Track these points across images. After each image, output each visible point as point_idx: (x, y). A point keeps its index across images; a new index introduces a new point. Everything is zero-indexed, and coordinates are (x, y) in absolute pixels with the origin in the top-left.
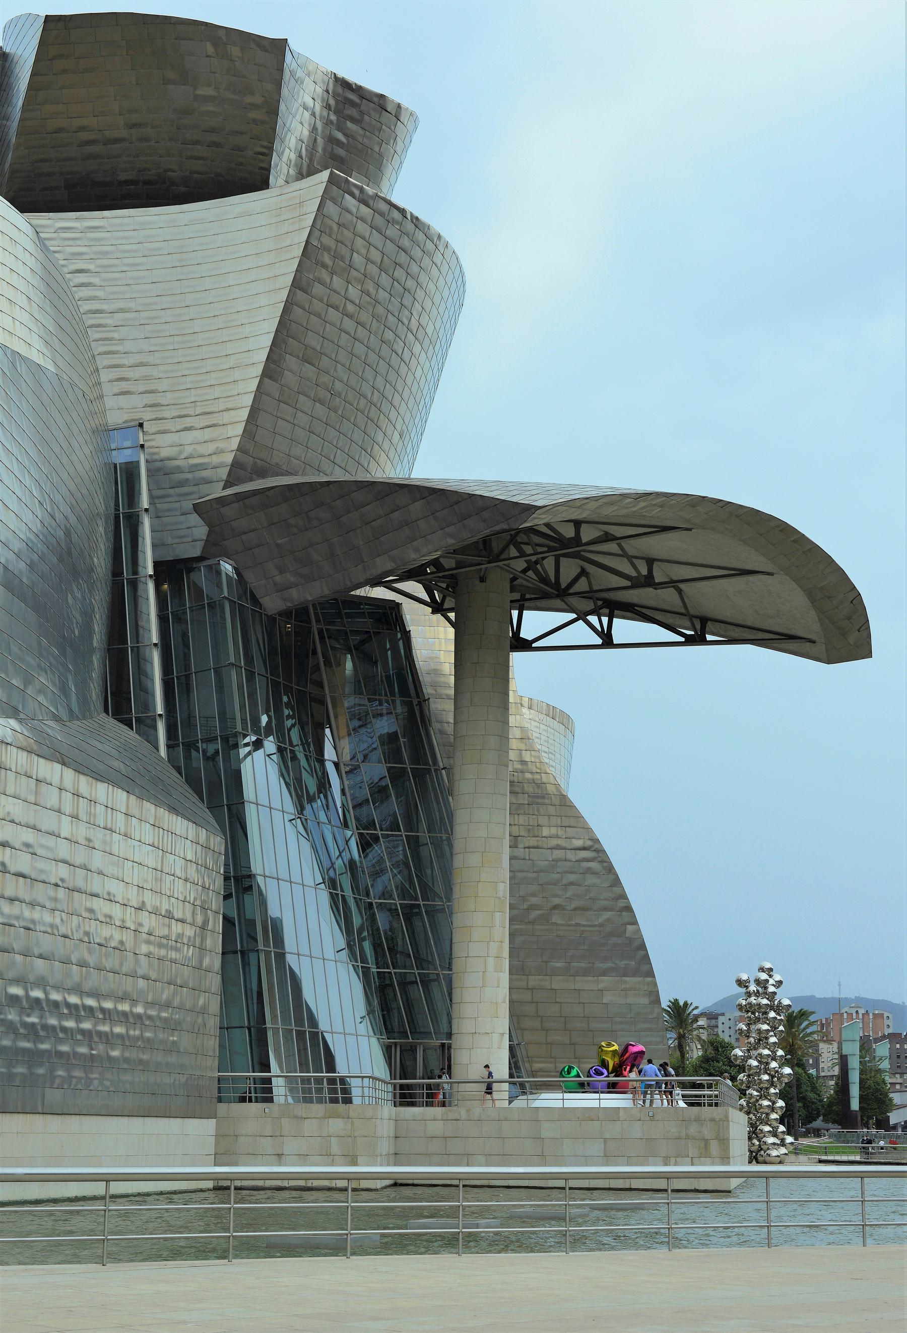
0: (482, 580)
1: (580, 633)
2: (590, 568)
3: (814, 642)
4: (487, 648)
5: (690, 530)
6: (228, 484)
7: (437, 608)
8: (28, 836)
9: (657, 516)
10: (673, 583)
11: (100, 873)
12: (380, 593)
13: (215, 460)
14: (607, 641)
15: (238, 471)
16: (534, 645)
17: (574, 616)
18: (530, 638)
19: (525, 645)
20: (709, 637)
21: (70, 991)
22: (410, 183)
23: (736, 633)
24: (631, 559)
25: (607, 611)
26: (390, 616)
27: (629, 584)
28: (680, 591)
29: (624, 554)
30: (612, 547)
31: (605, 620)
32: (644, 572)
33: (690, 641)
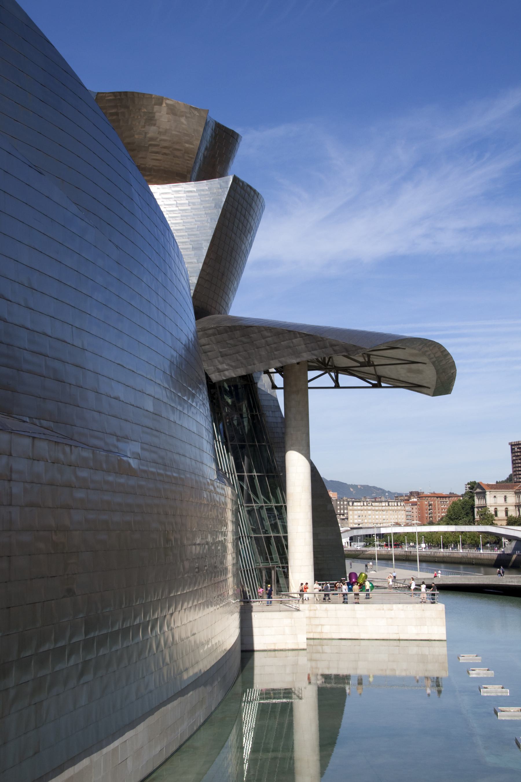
5: (405, 349)
14: (337, 386)
27: (359, 365)
32: (367, 359)
33: (374, 386)
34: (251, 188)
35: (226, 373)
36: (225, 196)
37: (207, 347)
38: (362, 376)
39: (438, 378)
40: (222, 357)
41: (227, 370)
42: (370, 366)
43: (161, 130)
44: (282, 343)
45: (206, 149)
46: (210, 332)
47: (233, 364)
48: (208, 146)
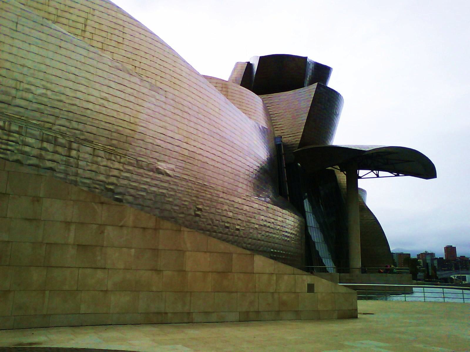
1: (372, 174)
4: (353, 179)
6: (299, 148)
7: (342, 170)
8: (273, 221)
11: (284, 227)
12: (330, 168)
14: (378, 176)
16: (362, 177)
17: (371, 171)
18: (361, 176)
19: (360, 178)
20: (400, 175)
21: (279, 250)
22: (332, 83)
26: (333, 172)
33: (396, 176)
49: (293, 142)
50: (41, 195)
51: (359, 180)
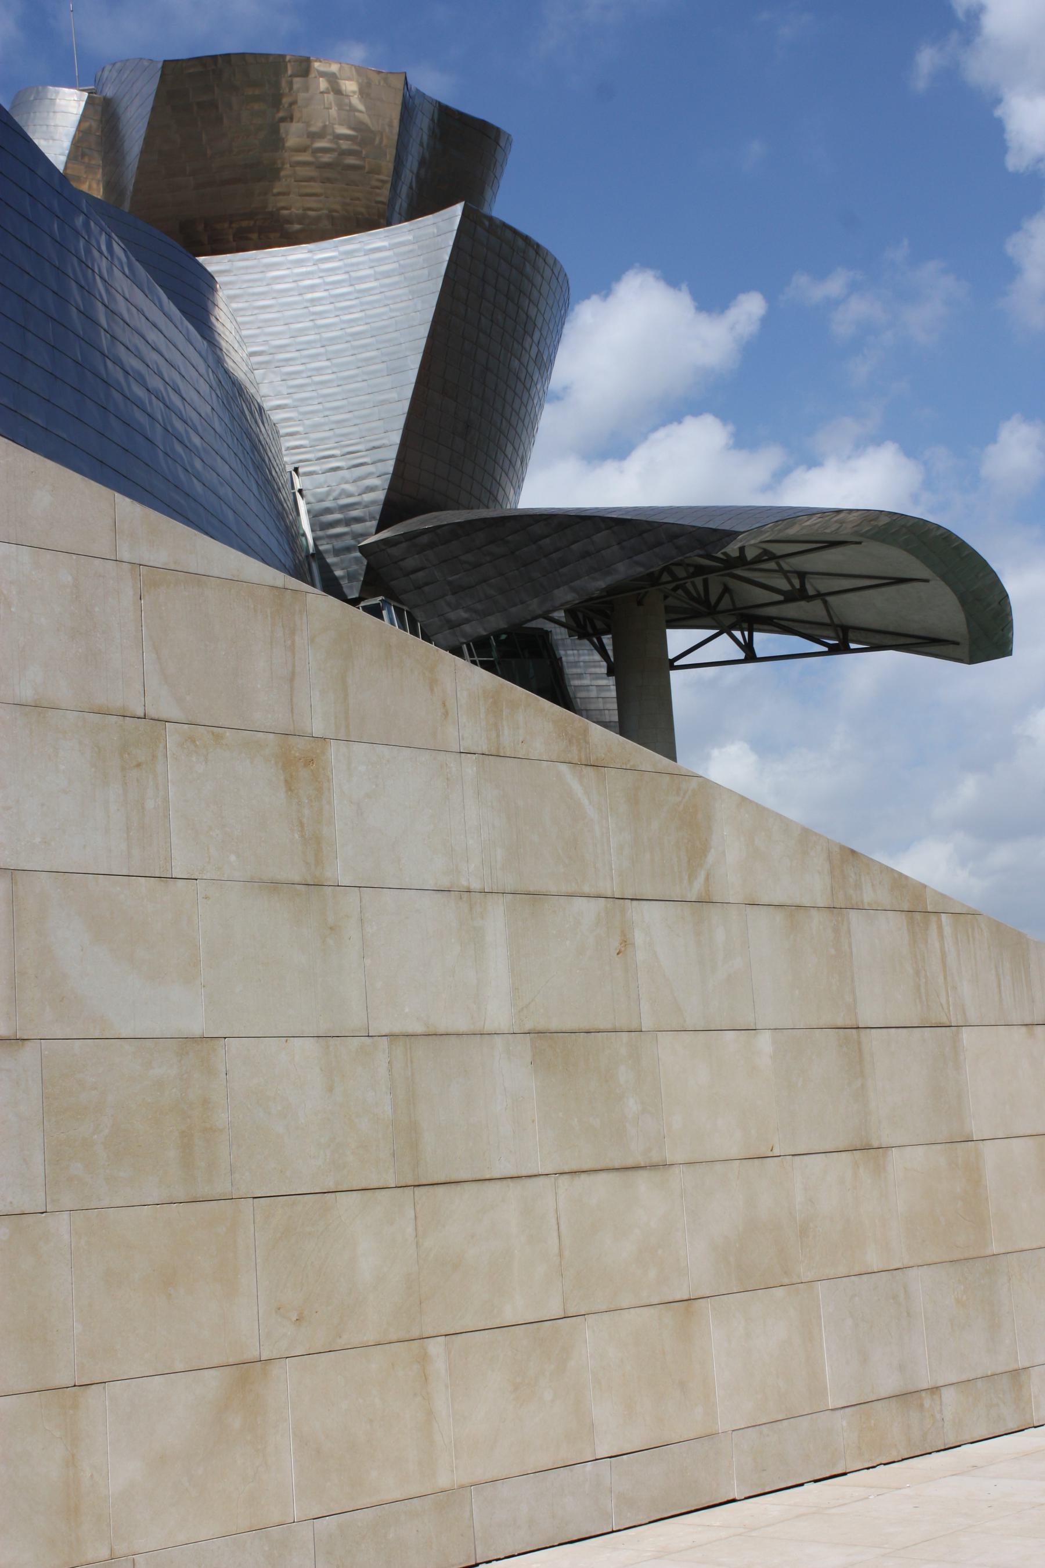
0: (640, 603)
1: (725, 647)
2: (733, 584)
3: (957, 644)
5: (860, 543)
9: (830, 532)
10: (820, 595)
13: (368, 497)
14: (751, 657)
15: (392, 511)
16: (676, 664)
19: (672, 665)
20: (853, 646)
23: (877, 639)
24: (785, 574)
25: (745, 625)
27: (781, 598)
28: (825, 603)
29: (781, 570)
30: (772, 565)
31: (746, 633)
32: (798, 587)
33: (833, 650)
34: (515, 232)
35: (467, 628)
36: (449, 250)
37: (421, 574)
38: (809, 632)
39: (969, 617)
40: (454, 594)
41: (467, 621)
42: (809, 598)
43: (313, 129)
44: (573, 547)
45: (422, 162)
46: (424, 539)
47: (479, 606)
48: (427, 155)
49: (351, 495)
50: (318, 728)
51: (673, 674)
